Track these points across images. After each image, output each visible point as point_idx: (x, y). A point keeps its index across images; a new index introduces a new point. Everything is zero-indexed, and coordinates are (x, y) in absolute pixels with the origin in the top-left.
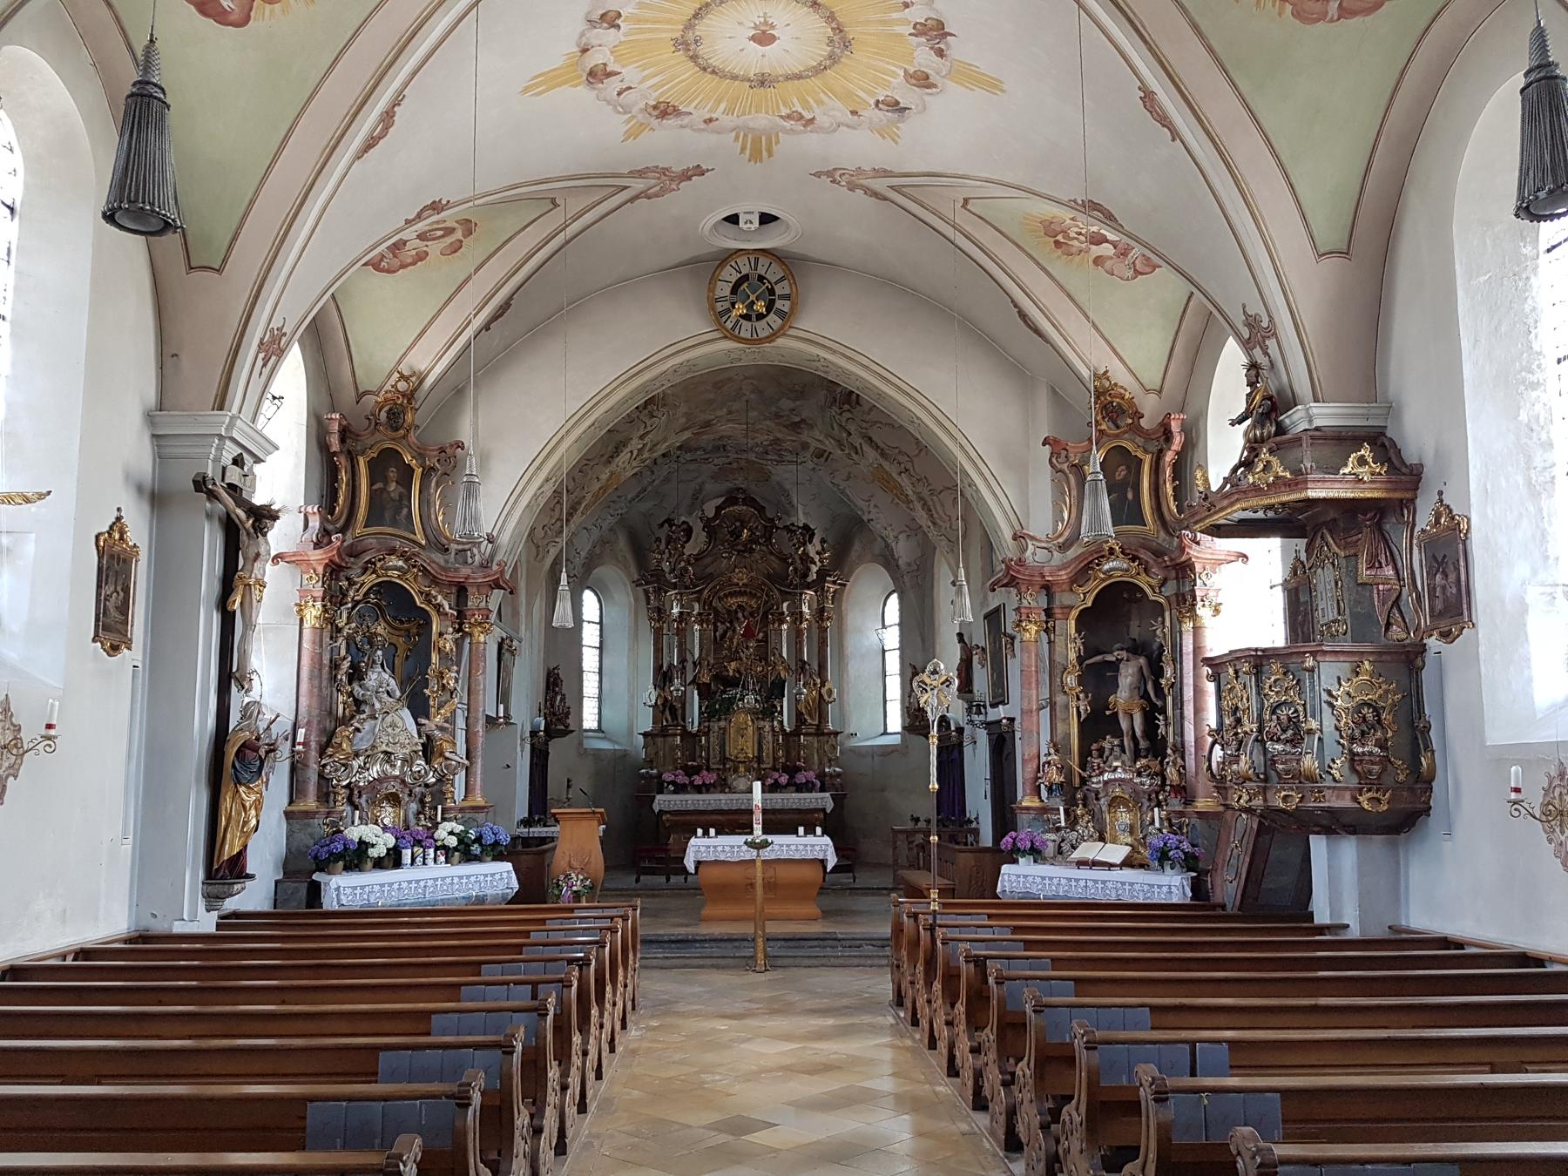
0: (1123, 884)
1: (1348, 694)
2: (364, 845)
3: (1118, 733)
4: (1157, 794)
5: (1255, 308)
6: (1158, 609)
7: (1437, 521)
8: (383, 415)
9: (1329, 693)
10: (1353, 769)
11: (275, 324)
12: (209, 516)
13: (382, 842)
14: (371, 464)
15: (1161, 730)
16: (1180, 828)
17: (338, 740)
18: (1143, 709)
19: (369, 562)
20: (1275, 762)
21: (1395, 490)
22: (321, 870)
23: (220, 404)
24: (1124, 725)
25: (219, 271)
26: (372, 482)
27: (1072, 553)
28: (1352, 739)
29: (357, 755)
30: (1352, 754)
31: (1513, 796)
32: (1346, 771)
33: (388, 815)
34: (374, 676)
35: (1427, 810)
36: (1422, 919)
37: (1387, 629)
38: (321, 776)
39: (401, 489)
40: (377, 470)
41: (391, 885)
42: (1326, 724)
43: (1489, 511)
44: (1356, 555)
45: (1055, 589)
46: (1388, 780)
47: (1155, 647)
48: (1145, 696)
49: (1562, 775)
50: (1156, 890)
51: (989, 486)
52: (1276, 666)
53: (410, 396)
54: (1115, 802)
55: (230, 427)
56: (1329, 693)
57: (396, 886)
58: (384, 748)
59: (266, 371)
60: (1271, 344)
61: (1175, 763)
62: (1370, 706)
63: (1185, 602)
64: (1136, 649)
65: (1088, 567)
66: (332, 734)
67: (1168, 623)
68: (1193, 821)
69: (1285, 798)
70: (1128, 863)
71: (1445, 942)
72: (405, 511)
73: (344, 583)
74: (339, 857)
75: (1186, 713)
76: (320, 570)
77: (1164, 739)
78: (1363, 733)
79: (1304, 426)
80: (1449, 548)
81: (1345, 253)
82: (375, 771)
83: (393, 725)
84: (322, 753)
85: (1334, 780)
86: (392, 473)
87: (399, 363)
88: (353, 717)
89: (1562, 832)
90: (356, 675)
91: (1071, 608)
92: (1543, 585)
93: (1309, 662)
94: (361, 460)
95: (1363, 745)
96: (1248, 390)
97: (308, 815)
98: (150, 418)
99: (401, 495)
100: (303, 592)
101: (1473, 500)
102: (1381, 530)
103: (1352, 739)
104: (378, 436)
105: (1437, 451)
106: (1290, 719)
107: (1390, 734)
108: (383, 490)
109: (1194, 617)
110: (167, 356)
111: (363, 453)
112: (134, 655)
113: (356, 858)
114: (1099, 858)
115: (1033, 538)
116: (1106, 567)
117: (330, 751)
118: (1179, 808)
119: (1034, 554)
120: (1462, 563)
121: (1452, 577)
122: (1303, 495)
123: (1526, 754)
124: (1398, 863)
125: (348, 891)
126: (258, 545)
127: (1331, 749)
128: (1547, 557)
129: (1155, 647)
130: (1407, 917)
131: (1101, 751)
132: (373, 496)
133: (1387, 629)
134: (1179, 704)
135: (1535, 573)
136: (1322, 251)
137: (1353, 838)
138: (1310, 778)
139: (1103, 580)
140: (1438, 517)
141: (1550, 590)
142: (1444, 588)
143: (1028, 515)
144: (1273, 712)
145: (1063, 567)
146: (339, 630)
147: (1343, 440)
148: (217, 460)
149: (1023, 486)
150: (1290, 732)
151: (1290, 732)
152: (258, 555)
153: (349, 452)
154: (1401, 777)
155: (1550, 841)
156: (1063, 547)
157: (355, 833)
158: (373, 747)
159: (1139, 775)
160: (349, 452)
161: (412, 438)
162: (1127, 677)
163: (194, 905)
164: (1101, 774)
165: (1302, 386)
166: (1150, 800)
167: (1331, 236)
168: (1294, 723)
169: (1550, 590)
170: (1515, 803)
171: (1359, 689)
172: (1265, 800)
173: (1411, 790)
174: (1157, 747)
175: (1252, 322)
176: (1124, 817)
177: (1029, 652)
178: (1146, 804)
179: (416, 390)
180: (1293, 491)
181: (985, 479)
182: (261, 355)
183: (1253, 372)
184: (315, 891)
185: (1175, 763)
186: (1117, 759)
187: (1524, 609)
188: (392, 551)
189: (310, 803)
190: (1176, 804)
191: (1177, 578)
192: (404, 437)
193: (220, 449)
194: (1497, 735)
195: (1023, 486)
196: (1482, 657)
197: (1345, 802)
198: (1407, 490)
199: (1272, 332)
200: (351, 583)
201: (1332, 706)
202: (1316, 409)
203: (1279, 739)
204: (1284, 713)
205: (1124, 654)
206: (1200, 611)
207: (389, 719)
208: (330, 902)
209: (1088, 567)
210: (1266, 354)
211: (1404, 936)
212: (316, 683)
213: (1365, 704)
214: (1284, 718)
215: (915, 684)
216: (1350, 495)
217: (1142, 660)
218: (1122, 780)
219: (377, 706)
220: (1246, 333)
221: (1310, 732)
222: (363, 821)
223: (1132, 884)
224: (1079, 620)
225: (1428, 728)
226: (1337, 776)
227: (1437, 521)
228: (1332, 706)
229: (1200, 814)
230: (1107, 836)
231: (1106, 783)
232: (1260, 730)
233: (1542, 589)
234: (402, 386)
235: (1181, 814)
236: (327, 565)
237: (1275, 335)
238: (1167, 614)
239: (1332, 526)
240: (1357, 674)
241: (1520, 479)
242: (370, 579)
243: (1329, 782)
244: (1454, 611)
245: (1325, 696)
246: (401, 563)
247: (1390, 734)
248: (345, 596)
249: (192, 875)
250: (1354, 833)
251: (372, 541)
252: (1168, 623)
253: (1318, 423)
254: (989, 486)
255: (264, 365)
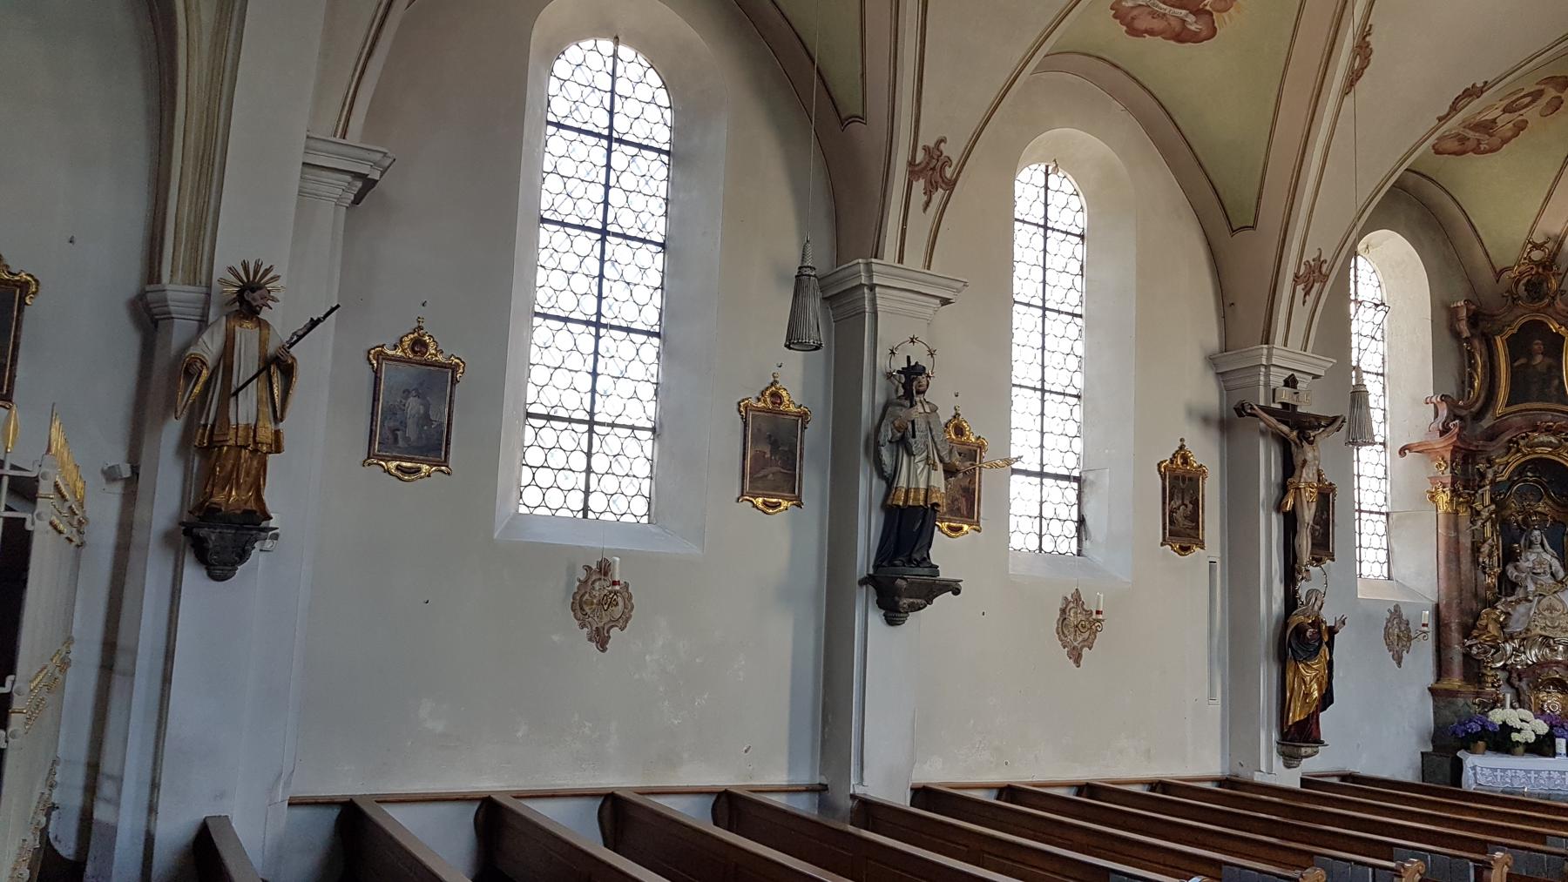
2: (1506, 729)
8: (1521, 287)
11: (1309, 256)
12: (1263, 433)
13: (1531, 727)
14: (1511, 343)
17: (1484, 622)
19: (1510, 441)
22: (1467, 749)
23: (1267, 340)
25: (1253, 227)
26: (1513, 357)
29: (1512, 638)
33: (1553, 701)
34: (1533, 557)
38: (1467, 656)
39: (1549, 361)
40: (1518, 347)
41: (1537, 772)
53: (1548, 264)
55: (1269, 356)
57: (1544, 775)
58: (1538, 631)
59: (1311, 299)
66: (1477, 617)
72: (1556, 382)
73: (1481, 466)
74: (1477, 737)
76: (1448, 456)
82: (1532, 656)
83: (1551, 608)
84: (1466, 632)
86: (1537, 345)
87: (1531, 232)
88: (1498, 599)
90: (1510, 557)
94: (1498, 339)
97: (1452, 694)
98: (1212, 360)
99: (1549, 368)
100: (1433, 480)
104: (1518, 312)
108: (1526, 365)
110: (1226, 304)
111: (1500, 332)
112: (1199, 558)
113: (1501, 740)
117: (1475, 633)
125: (1487, 772)
126: (1304, 453)
132: (1514, 374)
146: (1478, 513)
148: (1267, 384)
152: (1305, 461)
153: (1483, 334)
157: (1497, 716)
158: (1528, 630)
160: (1483, 334)
161: (1559, 305)
163: (1270, 761)
179: (1555, 255)
182: (1300, 288)
184: (1458, 766)
188: (1535, 429)
189: (1455, 682)
192: (1549, 305)
193: (1267, 375)
200: (1490, 462)
207: (1545, 602)
208: (1469, 783)
212: (1453, 567)
219: (1531, 588)
222: (1520, 702)
234: (1537, 255)
236: (1453, 453)
242: (1515, 460)
246: (1553, 439)
248: (1483, 476)
249: (1267, 737)
251: (1517, 419)
255: (1307, 293)
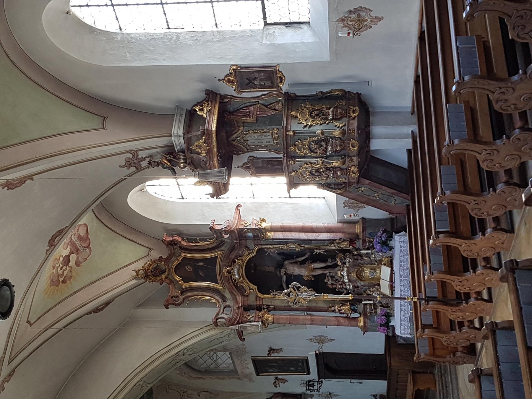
0: (401, 266)
1: (306, 120)
3: (324, 276)
4: (354, 255)
5: (122, 160)
6: (261, 251)
7: (232, 82)
9: (305, 127)
10: (340, 119)
15: (322, 252)
16: (371, 242)
18: (311, 263)
20: (336, 151)
21: (216, 101)
24: (319, 272)
27: (228, 295)
28: (326, 119)
30: (333, 119)
31: (351, 35)
32: (341, 122)
35: (359, 95)
36: (407, 101)
37: (277, 110)
42: (318, 129)
43: (229, 57)
44: (243, 123)
45: (246, 304)
46: (345, 108)
47: (279, 258)
48: (303, 263)
49: (343, 20)
50: (402, 249)
51: (186, 341)
52: (292, 149)
54: (360, 277)
56: (305, 127)
60: (141, 154)
61: (339, 243)
62: (311, 113)
63: (259, 234)
64: (280, 266)
65: (236, 286)
67: (268, 246)
68: (367, 235)
69: (353, 147)
70: (391, 264)
71: (417, 82)
75: (313, 238)
77: (327, 251)
78: (323, 115)
79: (182, 140)
80: (244, 77)
81: (105, 118)
85: (345, 125)
89: (367, 20)
91: (257, 296)
92: (262, 38)
93: (291, 133)
95: (329, 114)
96: (160, 166)
101: (224, 63)
102: (233, 112)
103: (326, 119)
105: (200, 81)
106: (317, 144)
107: (324, 106)
109: (265, 230)
114: (388, 278)
115: (218, 314)
116: (237, 277)
118: (361, 241)
119: (226, 314)
120: (251, 70)
121: (256, 75)
122: (214, 132)
123: (334, 39)
124: (381, 112)
127: (331, 126)
128: (251, 35)
129: (279, 258)
130: (407, 107)
131: (332, 284)
133: (277, 110)
134: (308, 242)
135: (257, 40)
136: (102, 127)
137: (371, 118)
138: (344, 133)
139: (244, 278)
140: (229, 81)
141: (265, 35)
142: (261, 80)
143: (205, 322)
144: (313, 152)
145: (235, 299)
147: (192, 118)
149: (191, 324)
150: (323, 143)
151: (323, 143)
154: (344, 103)
155: (371, 27)
156: (224, 299)
159: (345, 263)
162: (296, 270)
164: (344, 283)
165: (163, 141)
166: (357, 260)
167: (96, 122)
168: (318, 142)
169: (265, 35)
170: (354, 34)
171: (303, 117)
172: (354, 156)
173: (349, 100)
174: (331, 255)
175: (129, 164)
176: (367, 272)
177: (279, 319)
178: (360, 261)
180: (212, 136)
181: (182, 343)
183: (153, 163)
185: (339, 243)
186: (337, 274)
187: (273, 45)
190: (359, 244)
191: (246, 240)
194: (326, 56)
195: (191, 324)
196: (291, 62)
197: (355, 124)
198: (216, 96)
199: (135, 153)
201: (311, 126)
202: (174, 132)
203: (326, 148)
204: (314, 146)
205: (283, 270)
206: (264, 225)
209: (236, 286)
210: (144, 159)
211: (416, 110)
213: (310, 115)
214: (316, 146)
215: (295, 307)
216: (216, 116)
217: (286, 262)
218: (348, 272)
220: (133, 169)
221: (323, 133)
223: (401, 261)
224: (263, 293)
225: (322, 92)
226: (343, 125)
227: (232, 82)
228: (311, 126)
229: (364, 229)
230: (377, 282)
231: (350, 281)
232: (322, 158)
233: (265, 38)
235: (364, 241)
237: (137, 151)
238: (264, 246)
239: (229, 134)
240: (297, 117)
241: (217, 45)
243: (346, 127)
244: (269, 75)
245: (307, 128)
247: (324, 106)
250: (369, 126)
252: (268, 246)
253: (181, 133)
254: (186, 341)
